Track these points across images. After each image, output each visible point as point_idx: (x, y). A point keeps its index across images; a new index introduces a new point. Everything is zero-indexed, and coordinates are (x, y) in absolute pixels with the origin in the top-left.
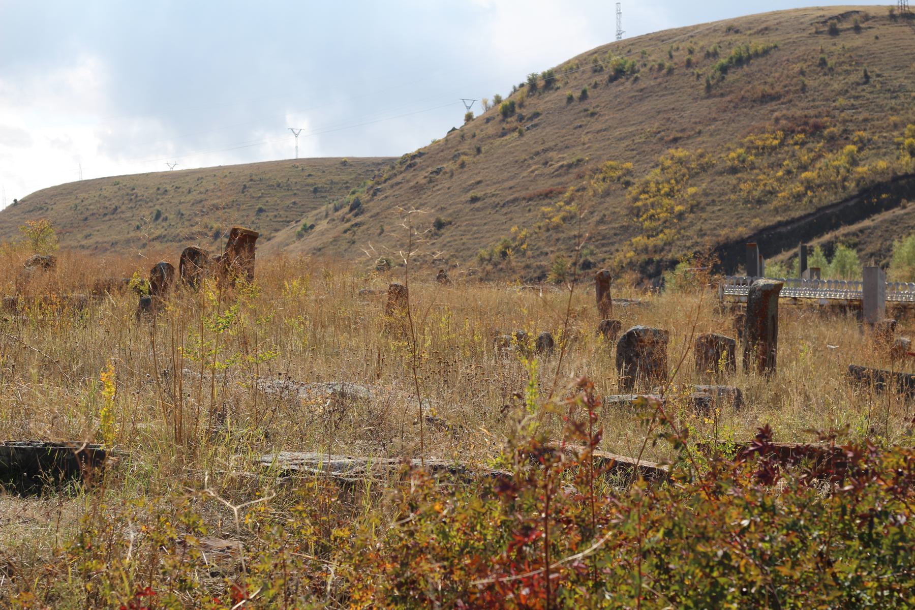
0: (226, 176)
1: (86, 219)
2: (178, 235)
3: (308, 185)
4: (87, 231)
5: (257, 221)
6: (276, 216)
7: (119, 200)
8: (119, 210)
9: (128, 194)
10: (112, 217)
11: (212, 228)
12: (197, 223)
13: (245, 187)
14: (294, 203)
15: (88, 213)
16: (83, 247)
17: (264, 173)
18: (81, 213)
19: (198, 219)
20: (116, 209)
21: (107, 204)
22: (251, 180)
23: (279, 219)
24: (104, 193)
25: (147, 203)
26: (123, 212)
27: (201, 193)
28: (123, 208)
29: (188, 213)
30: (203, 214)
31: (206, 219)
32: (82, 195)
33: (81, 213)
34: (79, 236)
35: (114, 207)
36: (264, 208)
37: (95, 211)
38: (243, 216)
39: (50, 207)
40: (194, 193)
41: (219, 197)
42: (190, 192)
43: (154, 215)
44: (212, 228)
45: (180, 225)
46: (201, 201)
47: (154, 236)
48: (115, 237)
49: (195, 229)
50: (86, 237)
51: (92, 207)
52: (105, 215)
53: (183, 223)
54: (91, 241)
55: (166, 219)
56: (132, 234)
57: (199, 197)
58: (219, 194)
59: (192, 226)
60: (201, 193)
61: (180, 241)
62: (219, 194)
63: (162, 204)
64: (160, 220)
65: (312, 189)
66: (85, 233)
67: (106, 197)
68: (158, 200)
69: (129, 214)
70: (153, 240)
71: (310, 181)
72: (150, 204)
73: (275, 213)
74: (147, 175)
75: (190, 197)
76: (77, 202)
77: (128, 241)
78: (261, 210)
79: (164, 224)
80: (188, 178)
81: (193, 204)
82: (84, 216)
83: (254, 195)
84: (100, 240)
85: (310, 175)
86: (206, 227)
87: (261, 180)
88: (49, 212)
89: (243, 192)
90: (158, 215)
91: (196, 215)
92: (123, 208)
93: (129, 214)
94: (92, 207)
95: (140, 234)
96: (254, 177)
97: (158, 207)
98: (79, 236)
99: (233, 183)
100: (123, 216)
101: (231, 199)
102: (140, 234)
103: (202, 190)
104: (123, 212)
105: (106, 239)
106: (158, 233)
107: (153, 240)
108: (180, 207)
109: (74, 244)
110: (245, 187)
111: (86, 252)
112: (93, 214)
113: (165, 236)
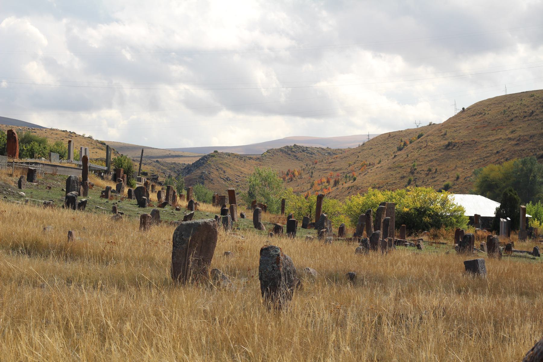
1: (512, 120)
4: (513, 128)
7: (534, 107)
8: (535, 114)
10: (529, 118)
15: (513, 116)
16: (510, 139)
18: (508, 116)
20: (533, 112)
21: (526, 110)
26: (537, 115)
33: (508, 116)
34: (508, 132)
35: (531, 111)
37: (518, 115)
50: (512, 132)
52: (525, 117)
54: (516, 135)
66: (511, 129)
82: (510, 118)
84: (522, 134)
92: (538, 111)
100: (537, 117)
109: (504, 137)
112: (516, 117)
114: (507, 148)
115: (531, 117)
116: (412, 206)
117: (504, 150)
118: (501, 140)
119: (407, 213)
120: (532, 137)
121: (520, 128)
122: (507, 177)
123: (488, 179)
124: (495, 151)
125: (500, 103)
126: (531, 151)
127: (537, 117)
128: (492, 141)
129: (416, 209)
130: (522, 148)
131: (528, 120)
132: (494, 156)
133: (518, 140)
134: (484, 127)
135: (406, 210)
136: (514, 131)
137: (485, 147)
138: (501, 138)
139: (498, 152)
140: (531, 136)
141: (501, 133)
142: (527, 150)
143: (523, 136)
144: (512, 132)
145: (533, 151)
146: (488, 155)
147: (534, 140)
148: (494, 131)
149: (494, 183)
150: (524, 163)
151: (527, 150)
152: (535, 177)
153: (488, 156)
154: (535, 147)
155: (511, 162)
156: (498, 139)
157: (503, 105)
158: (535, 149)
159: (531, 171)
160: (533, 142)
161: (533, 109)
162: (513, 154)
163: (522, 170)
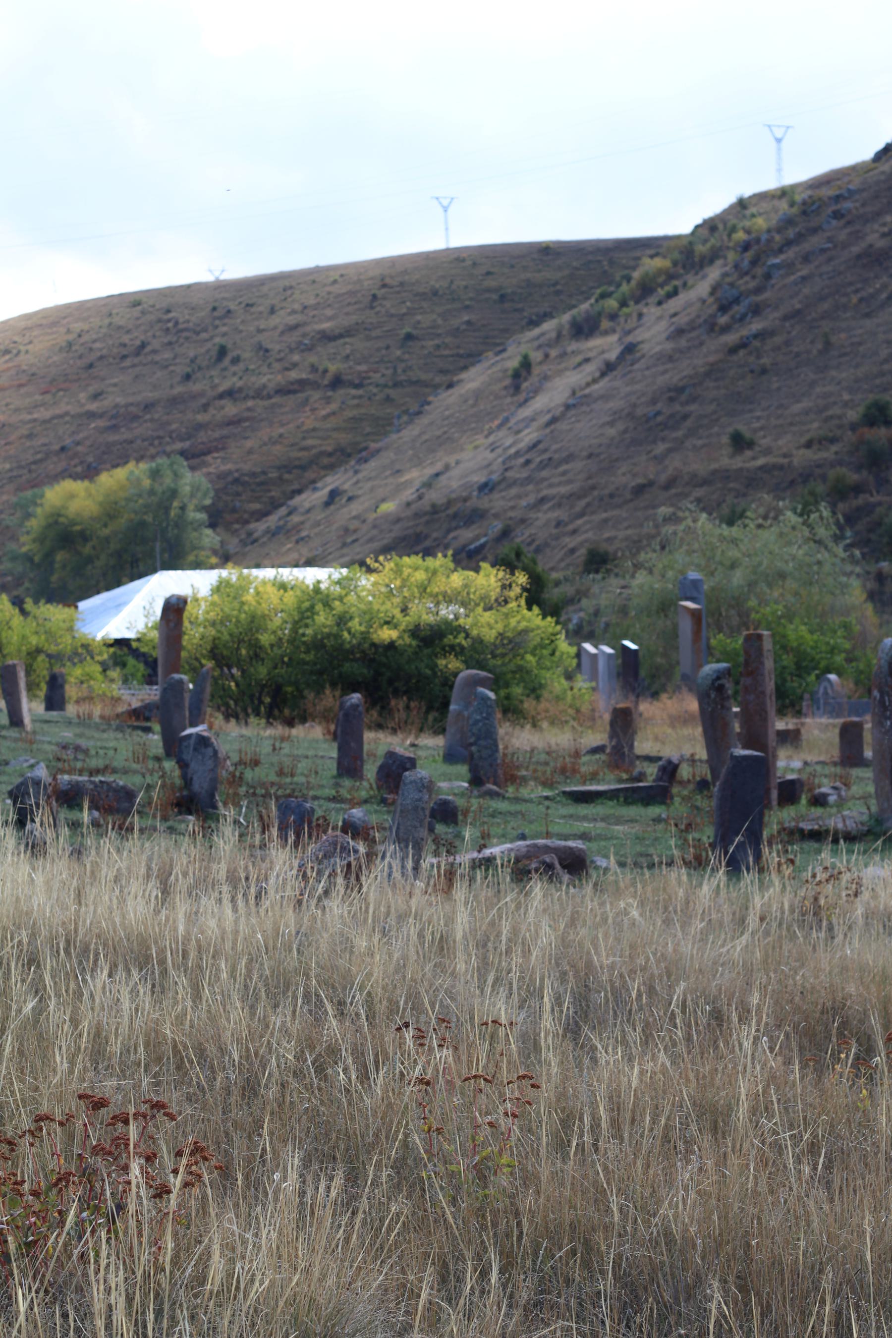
0: (335, 282)
1: (91, 366)
2: (265, 386)
3: (488, 290)
5: (407, 356)
6: (438, 347)
7: (146, 332)
8: (148, 349)
9: (160, 321)
10: (136, 360)
11: (326, 371)
12: (295, 365)
13: (374, 297)
14: (469, 323)
16: (91, 415)
17: (405, 272)
19: (296, 358)
20: (143, 345)
21: (126, 339)
22: (384, 286)
23: (447, 352)
24: (117, 321)
25: (197, 333)
26: (154, 352)
27: (294, 312)
28: (155, 344)
29: (277, 347)
30: (310, 349)
31: (313, 359)
32: (78, 326)
33: (81, 357)
34: (82, 396)
35: (138, 343)
36: (415, 332)
37: (105, 352)
38: (378, 350)
39: (22, 348)
40: (282, 312)
41: (330, 319)
42: (272, 311)
43: (214, 353)
44: (326, 371)
45: (264, 369)
46: (296, 327)
47: (221, 389)
48: (151, 395)
49: (294, 375)
50: (96, 396)
51: (97, 345)
52: (124, 357)
53: (269, 366)
55: (236, 360)
56: (178, 390)
57: (292, 320)
58: (329, 312)
59: (287, 369)
60: (294, 312)
61: (269, 397)
62: (329, 312)
63: (224, 335)
64: (227, 361)
65: (495, 297)
66: (91, 390)
67: (120, 328)
68: (217, 327)
69: (167, 355)
70: (221, 396)
71: (491, 283)
72: (204, 335)
73: (437, 342)
74: (189, 287)
75: (275, 320)
76: (71, 337)
77: (174, 401)
78: (409, 337)
79: (234, 368)
80: (265, 289)
81: (282, 333)
83: (393, 311)
84: (120, 400)
85: (488, 273)
86: (314, 369)
87: (402, 284)
88: (22, 357)
89: (372, 308)
90: (222, 352)
91: (292, 350)
92: (155, 344)
93: (167, 355)
94: (97, 345)
95: (195, 387)
96: (388, 281)
97: (217, 340)
98: (82, 396)
99: (351, 293)
100: (157, 358)
101: (354, 318)
102: (195, 387)
103: (297, 306)
104: (154, 352)
105: (131, 399)
106: (224, 386)
107: (221, 396)
108: (261, 337)
110: (374, 297)
111: (102, 423)
112: (101, 358)
113: (240, 390)
114: (86, 438)
115: (141, 358)
116: (406, 622)
117: (78, 444)
118: (67, 419)
119: (391, 645)
120: (148, 407)
121: (115, 385)
122: (110, 512)
123: (62, 520)
124: (57, 447)
125: (54, 324)
126: (151, 445)
127: (157, 358)
128: (45, 422)
129: (415, 631)
130: (125, 437)
131: (134, 366)
132: (55, 459)
133: (113, 417)
134: (21, 386)
135: (387, 634)
136: (100, 394)
137: (30, 436)
138: (67, 414)
139: (63, 449)
140: (146, 407)
141: (66, 400)
142: (139, 442)
143: (127, 406)
144: (96, 396)
145: (156, 442)
146: (39, 456)
147: (156, 416)
148: (48, 397)
149: (78, 528)
150: (155, 474)
151: (139, 442)
152: (183, 508)
153: (41, 461)
154: (161, 433)
155: (121, 473)
156: (61, 416)
157: (63, 330)
158: (159, 437)
159: (174, 493)
160: (152, 420)
161: (142, 337)
162: (104, 453)
163: (152, 492)
